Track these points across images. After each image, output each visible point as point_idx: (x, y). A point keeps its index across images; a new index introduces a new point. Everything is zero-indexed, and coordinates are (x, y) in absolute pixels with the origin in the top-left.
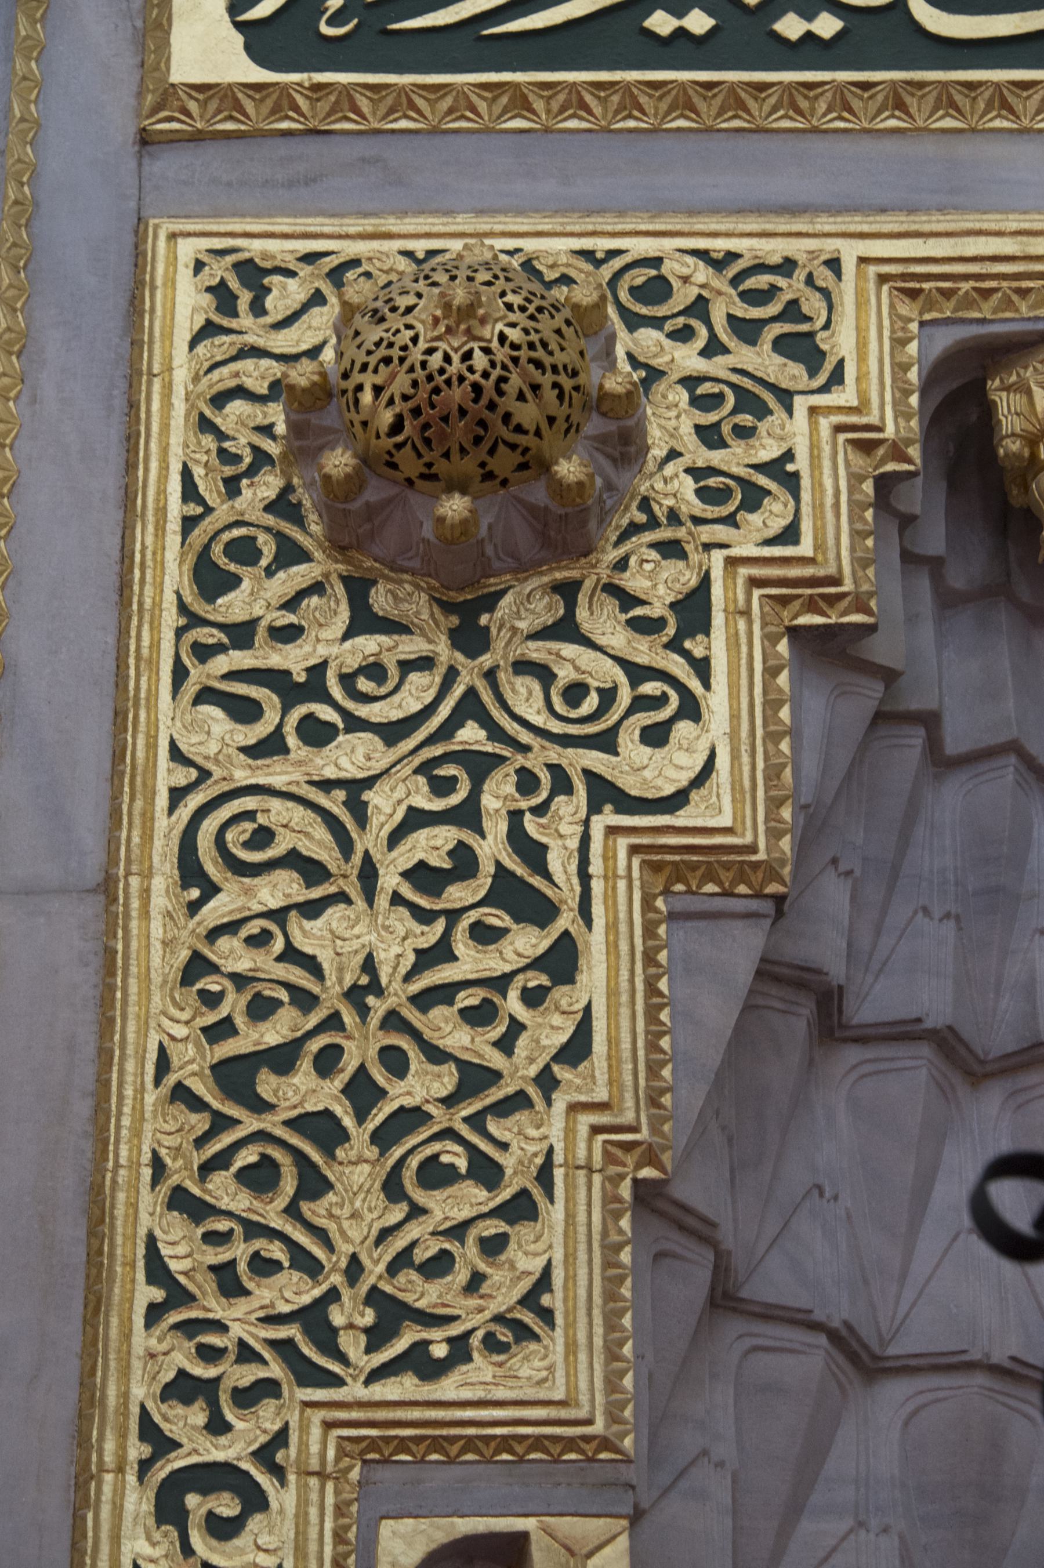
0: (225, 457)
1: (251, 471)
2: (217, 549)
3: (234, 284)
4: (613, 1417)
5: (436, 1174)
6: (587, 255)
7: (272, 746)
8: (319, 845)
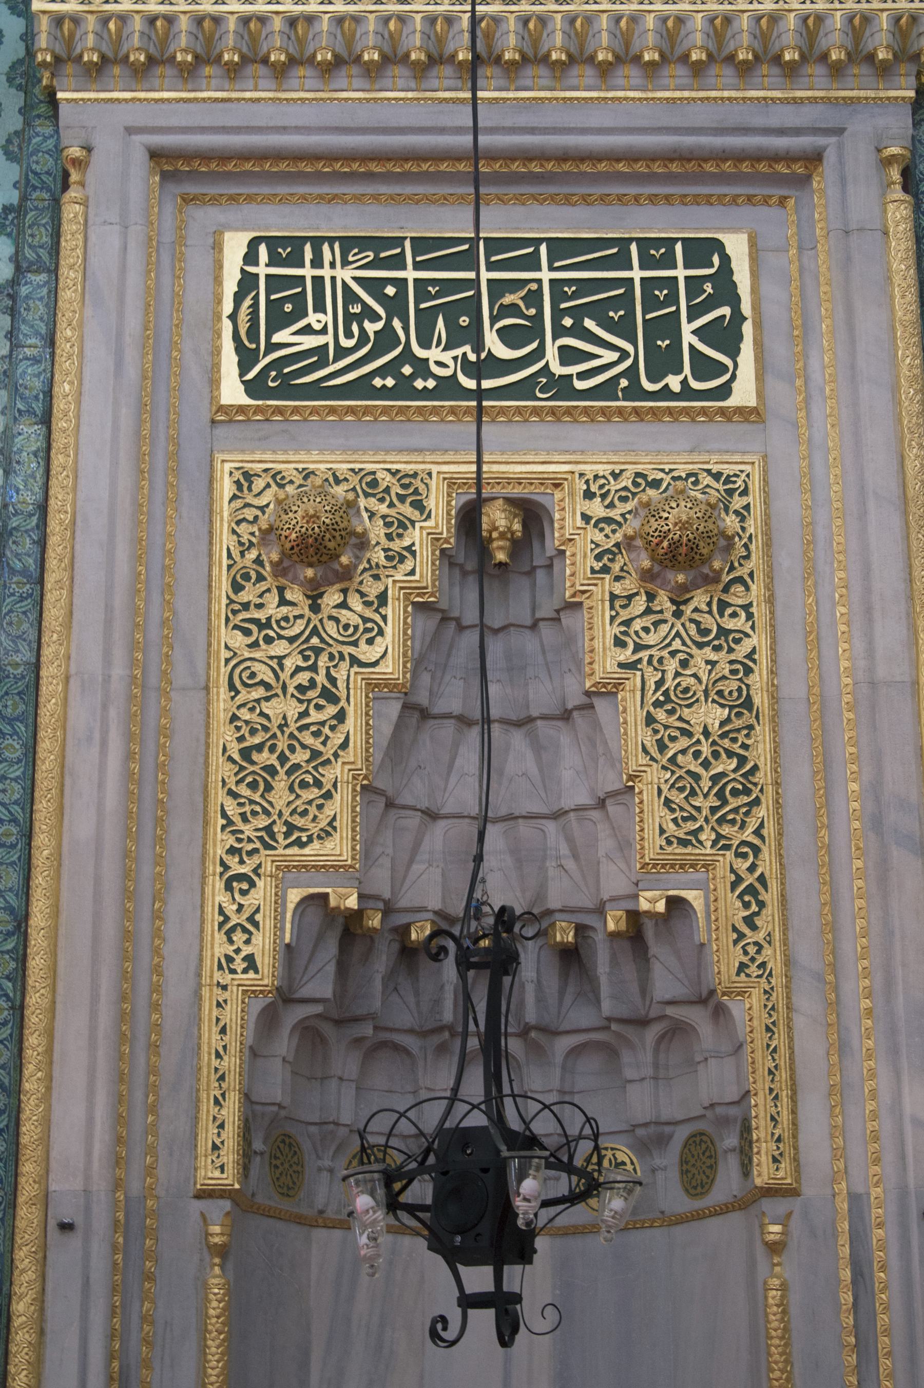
0: (241, 544)
1: (248, 548)
2: (238, 576)
3: (242, 480)
4: (353, 859)
5: (304, 785)
6: (352, 470)
7: (255, 645)
8: (269, 678)
